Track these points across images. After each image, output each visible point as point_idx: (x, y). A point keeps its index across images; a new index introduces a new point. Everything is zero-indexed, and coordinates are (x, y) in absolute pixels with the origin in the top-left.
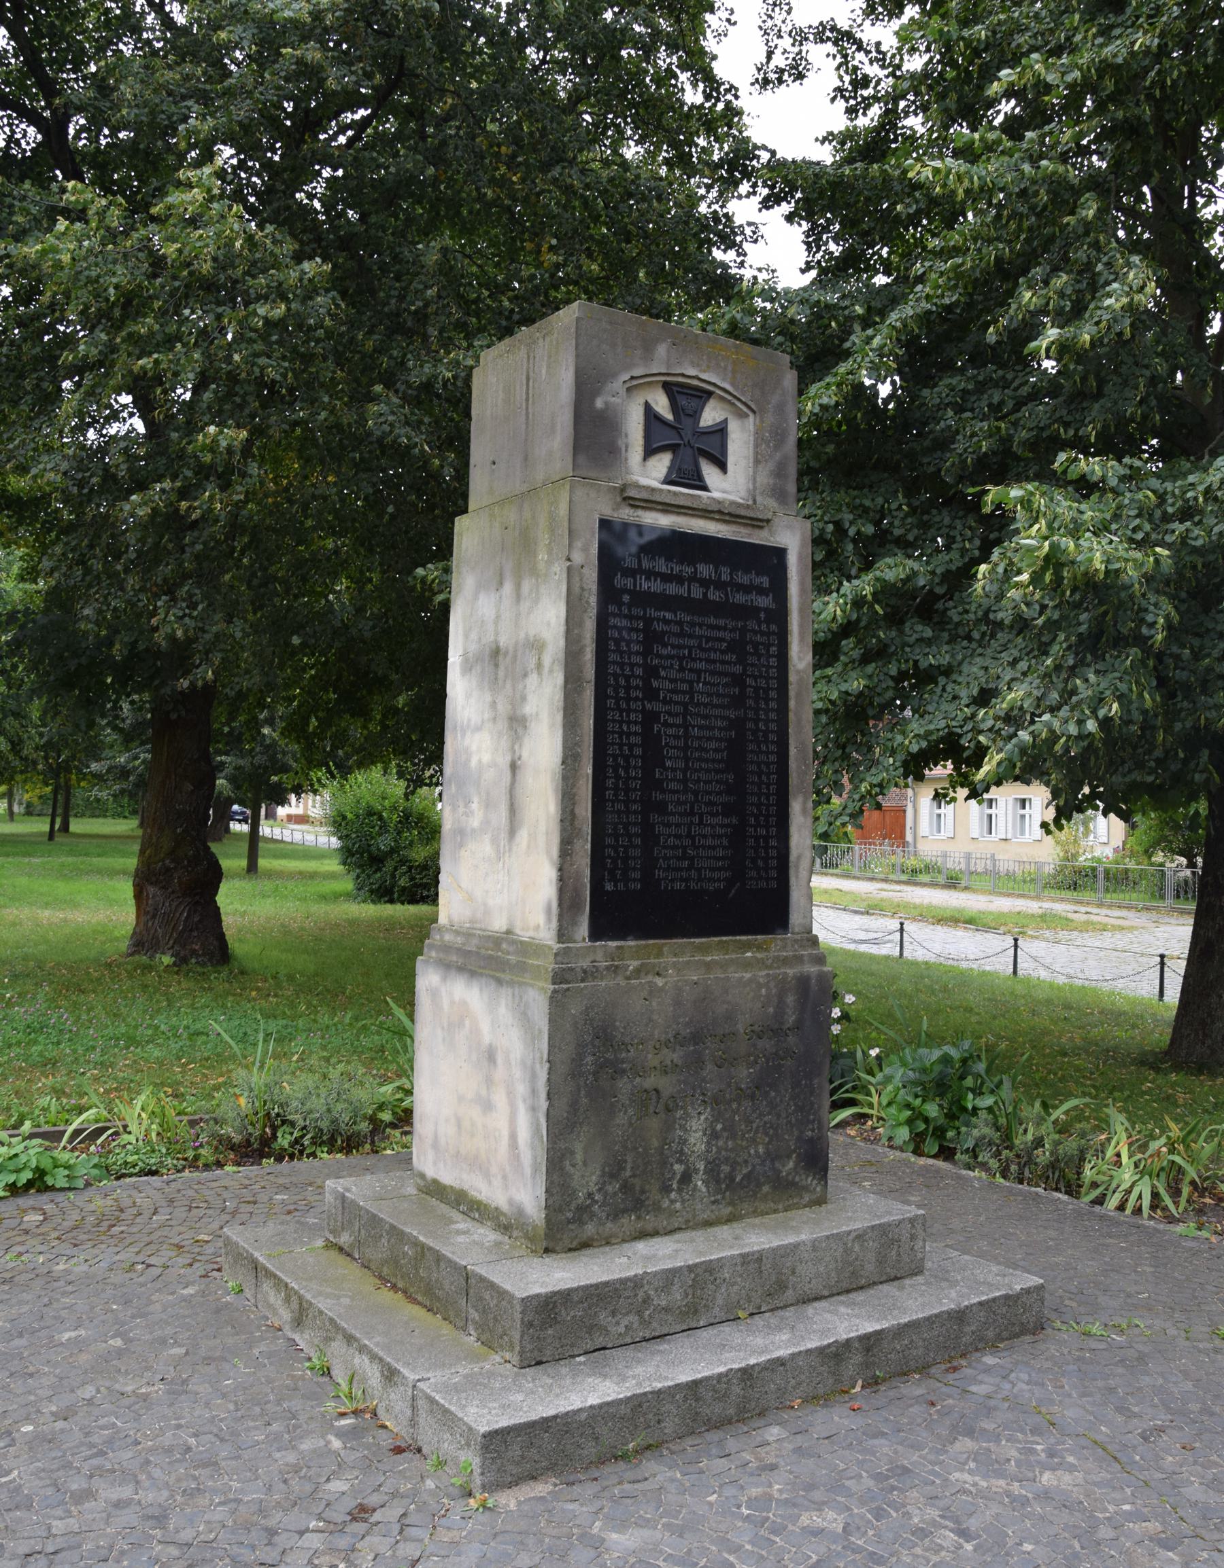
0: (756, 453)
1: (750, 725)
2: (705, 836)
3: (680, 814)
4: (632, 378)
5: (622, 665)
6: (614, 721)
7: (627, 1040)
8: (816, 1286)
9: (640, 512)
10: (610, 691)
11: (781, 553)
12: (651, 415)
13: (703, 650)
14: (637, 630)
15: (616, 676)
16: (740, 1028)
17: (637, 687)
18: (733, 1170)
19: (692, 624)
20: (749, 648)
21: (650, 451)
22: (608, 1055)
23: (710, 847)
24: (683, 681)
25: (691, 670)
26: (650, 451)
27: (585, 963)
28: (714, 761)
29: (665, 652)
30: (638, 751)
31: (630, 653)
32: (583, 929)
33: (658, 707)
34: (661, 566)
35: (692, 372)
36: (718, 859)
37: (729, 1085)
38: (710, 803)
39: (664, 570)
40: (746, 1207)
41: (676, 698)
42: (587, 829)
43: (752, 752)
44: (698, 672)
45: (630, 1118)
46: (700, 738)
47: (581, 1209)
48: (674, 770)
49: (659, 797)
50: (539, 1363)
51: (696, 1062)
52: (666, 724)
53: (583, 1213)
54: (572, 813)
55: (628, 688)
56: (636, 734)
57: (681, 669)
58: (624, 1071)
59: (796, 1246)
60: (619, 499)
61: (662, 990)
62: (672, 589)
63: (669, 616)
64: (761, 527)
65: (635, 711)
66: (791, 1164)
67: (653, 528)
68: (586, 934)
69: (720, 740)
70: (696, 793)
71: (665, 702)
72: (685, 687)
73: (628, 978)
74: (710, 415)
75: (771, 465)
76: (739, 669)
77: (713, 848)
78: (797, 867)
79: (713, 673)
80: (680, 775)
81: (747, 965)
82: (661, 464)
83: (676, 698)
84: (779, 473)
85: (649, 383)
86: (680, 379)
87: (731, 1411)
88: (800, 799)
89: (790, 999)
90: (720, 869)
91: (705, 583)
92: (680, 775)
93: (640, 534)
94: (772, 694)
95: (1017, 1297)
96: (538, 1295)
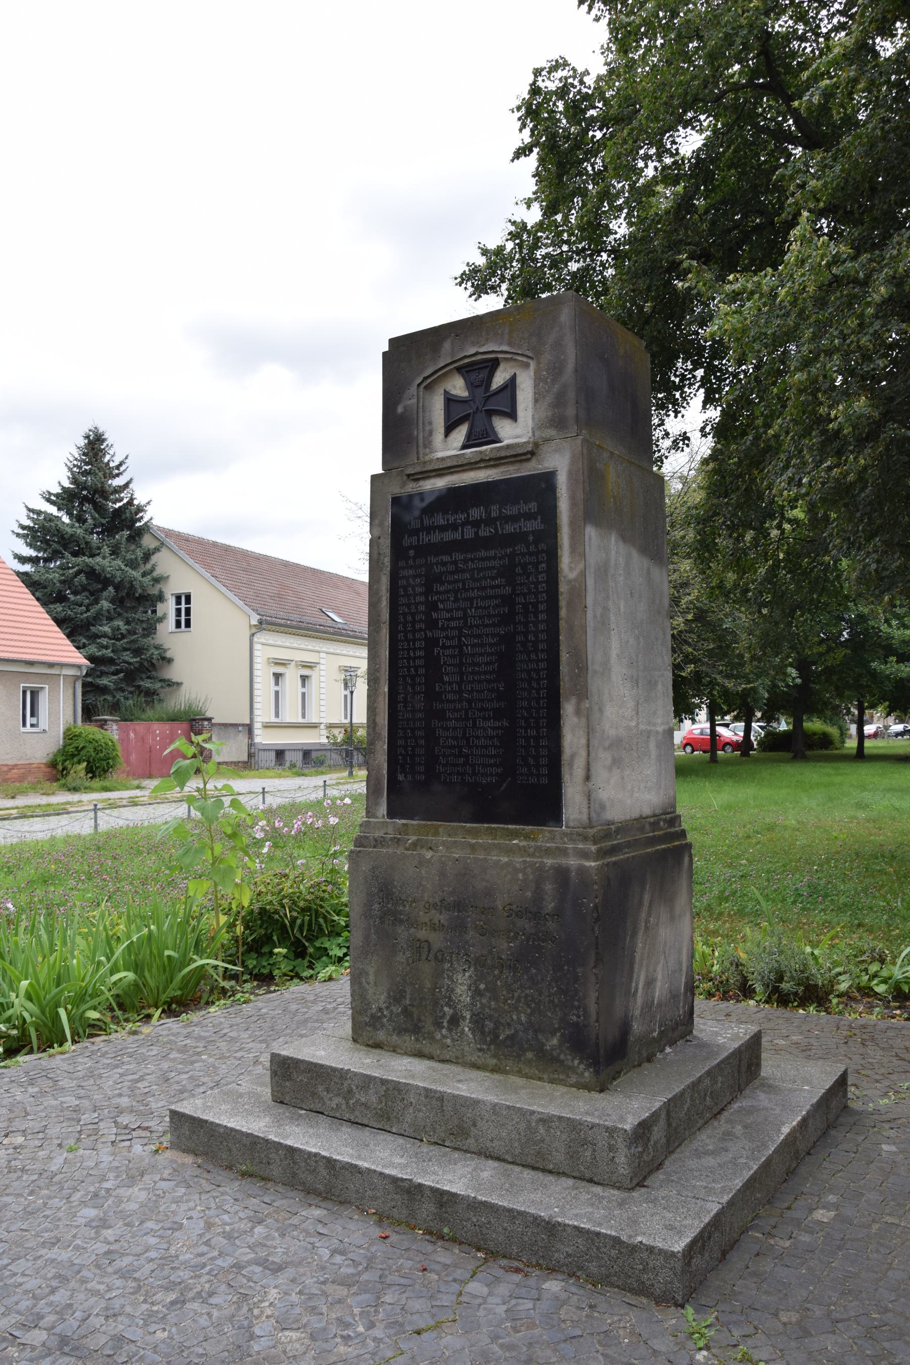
0: (535, 393)
1: (520, 638)
2: (478, 738)
3: (456, 719)
4: (425, 378)
5: (408, 605)
6: (403, 650)
7: (403, 897)
8: (497, 1146)
9: (421, 483)
10: (400, 627)
11: (549, 478)
12: (450, 400)
13: (475, 580)
14: (420, 576)
15: (404, 614)
16: (499, 904)
17: (421, 621)
18: (496, 1028)
19: (465, 561)
20: (518, 570)
21: (449, 429)
22: (390, 906)
23: (482, 747)
24: (458, 609)
25: (465, 599)
26: (449, 429)
27: (378, 834)
28: (485, 673)
29: (442, 589)
30: (422, 671)
31: (415, 595)
32: (383, 809)
33: (438, 634)
34: (440, 520)
35: (472, 351)
36: (491, 757)
37: (490, 952)
38: (482, 709)
39: (442, 522)
40: (509, 1065)
41: (453, 624)
42: (385, 733)
43: (521, 661)
44: (471, 600)
45: (407, 959)
46: (473, 655)
47: (373, 1016)
48: (450, 683)
49: (439, 706)
50: (282, 1102)
51: (459, 927)
52: (444, 647)
53: (375, 1021)
54: (374, 720)
55: (414, 622)
56: (420, 657)
57: (456, 600)
58: (401, 922)
59: (476, 1102)
60: (405, 478)
61: (429, 861)
62: (448, 536)
63: (446, 558)
64: (528, 460)
65: (419, 640)
66: (555, 1041)
67: (432, 492)
68: (385, 813)
69: (491, 654)
70: (469, 701)
71: (443, 629)
72: (460, 614)
73: (407, 849)
74: (499, 379)
75: (549, 399)
76: (508, 590)
77: (486, 747)
78: (571, 765)
79: (483, 598)
80: (455, 687)
81: (510, 851)
82: (460, 434)
83: (453, 624)
84: (559, 402)
85: (445, 375)
86: (467, 361)
87: (321, 1187)
88: (573, 701)
89: (549, 887)
90: (492, 766)
91: (476, 524)
92: (455, 687)
93: (422, 500)
94: (542, 607)
95: (634, 1249)
96: (279, 1055)
